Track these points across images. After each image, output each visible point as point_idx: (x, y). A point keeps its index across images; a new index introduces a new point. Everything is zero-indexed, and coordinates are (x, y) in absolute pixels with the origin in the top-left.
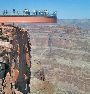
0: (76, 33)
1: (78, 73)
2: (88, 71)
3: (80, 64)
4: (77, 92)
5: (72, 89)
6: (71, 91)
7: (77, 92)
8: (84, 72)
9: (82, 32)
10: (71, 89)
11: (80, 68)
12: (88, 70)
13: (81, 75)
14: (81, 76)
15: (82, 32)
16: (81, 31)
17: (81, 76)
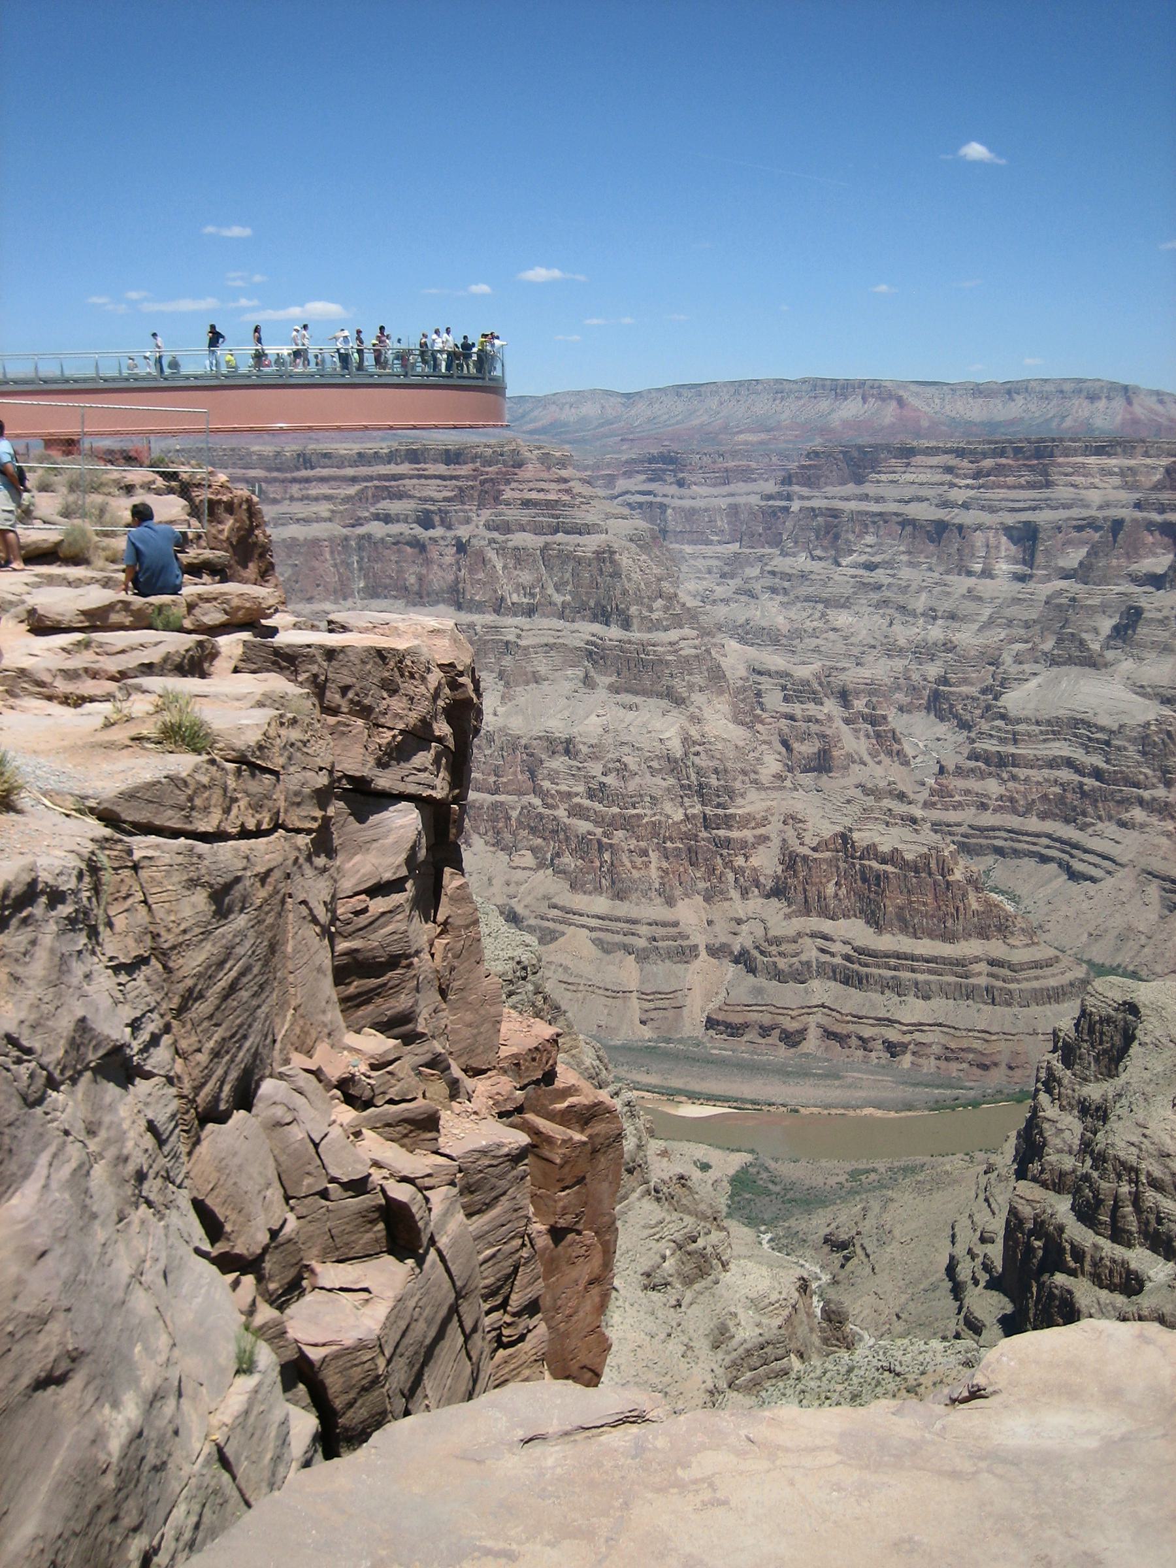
0: (534, 495)
1: (553, 777)
2: (625, 759)
3: (566, 713)
4: (555, 907)
5: (522, 889)
6: (513, 902)
7: (555, 907)
8: (596, 769)
9: (578, 487)
10: (512, 890)
11: (569, 741)
12: (626, 749)
13: (575, 789)
14: (577, 795)
15: (571, 484)
16: (565, 481)
17: (577, 800)
